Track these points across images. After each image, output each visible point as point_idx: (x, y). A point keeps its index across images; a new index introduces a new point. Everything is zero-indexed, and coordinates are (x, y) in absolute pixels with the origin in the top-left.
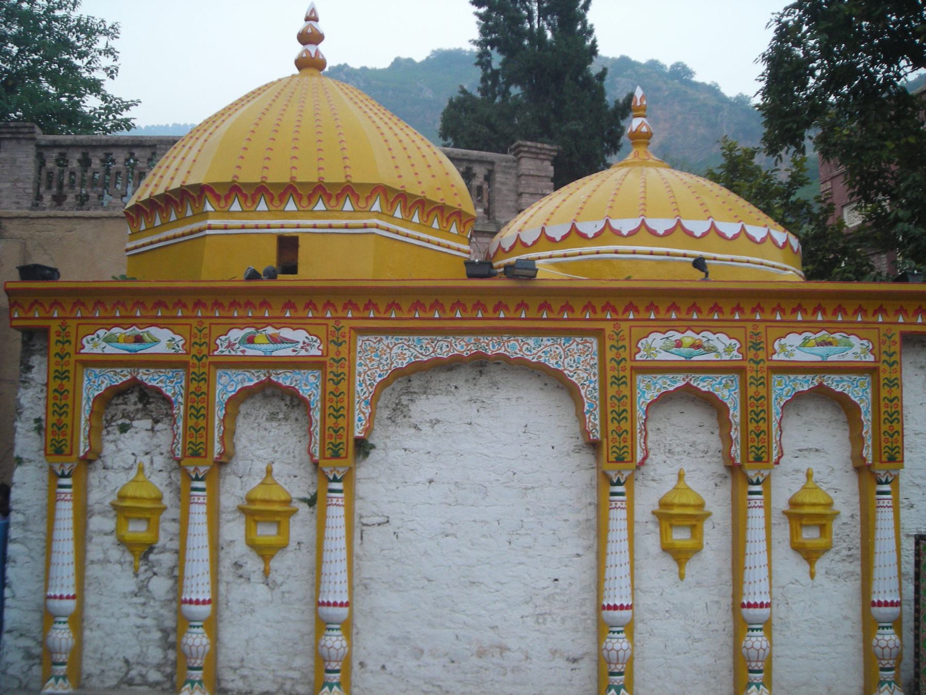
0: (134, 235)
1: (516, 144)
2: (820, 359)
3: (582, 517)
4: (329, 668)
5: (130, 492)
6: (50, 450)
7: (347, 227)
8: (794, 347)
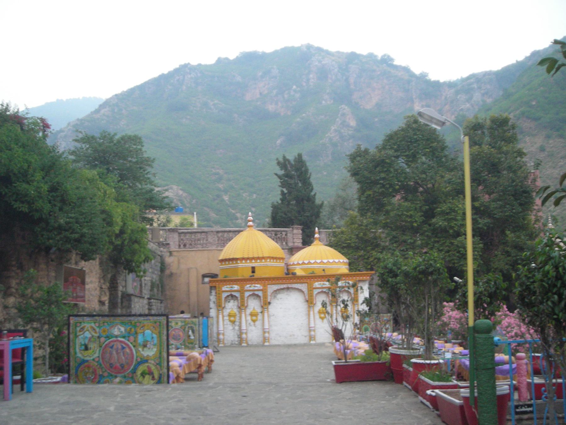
0: (222, 265)
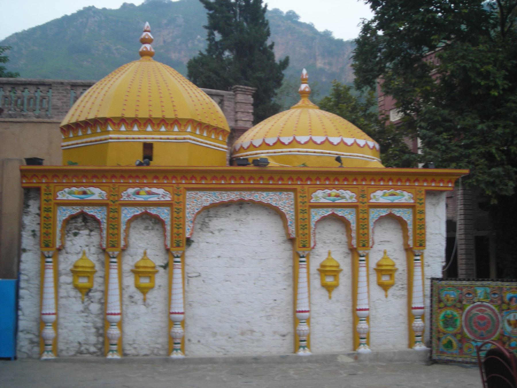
0: (67, 139)
1: (234, 87)
2: (390, 201)
3: (286, 272)
4: (176, 342)
5: (81, 264)
6: (43, 245)
7: (176, 139)
8: (380, 196)
